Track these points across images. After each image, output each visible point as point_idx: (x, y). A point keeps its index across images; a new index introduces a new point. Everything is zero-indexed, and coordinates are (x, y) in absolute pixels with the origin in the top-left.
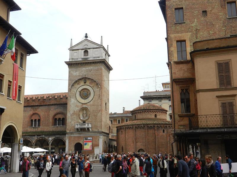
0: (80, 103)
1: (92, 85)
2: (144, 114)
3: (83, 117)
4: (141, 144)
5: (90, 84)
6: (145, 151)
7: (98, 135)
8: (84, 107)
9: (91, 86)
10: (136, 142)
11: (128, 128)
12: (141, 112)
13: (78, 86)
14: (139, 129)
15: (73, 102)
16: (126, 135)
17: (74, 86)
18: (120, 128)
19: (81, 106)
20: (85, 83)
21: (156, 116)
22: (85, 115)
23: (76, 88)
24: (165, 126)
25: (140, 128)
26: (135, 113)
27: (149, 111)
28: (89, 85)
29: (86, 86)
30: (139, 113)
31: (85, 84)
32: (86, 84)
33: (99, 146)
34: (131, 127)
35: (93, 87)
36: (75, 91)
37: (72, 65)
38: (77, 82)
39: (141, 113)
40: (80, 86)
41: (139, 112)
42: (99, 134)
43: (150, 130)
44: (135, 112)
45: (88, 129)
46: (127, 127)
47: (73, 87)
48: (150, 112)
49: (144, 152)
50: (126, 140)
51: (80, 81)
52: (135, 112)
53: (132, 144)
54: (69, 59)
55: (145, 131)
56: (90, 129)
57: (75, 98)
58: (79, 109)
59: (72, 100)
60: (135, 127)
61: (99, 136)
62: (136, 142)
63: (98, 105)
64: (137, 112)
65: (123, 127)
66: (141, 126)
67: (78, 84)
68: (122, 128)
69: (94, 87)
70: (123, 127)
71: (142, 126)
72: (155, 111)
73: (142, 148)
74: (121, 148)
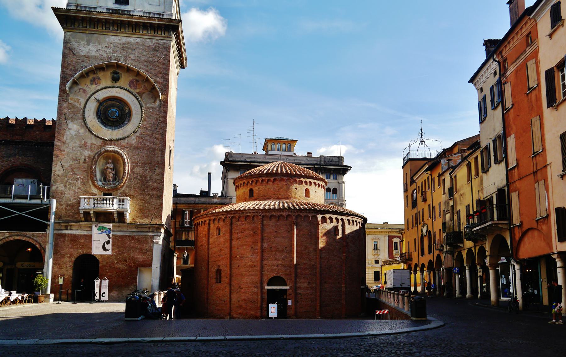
0: (95, 135)
1: (138, 91)
3: (105, 179)
5: (130, 86)
6: (288, 283)
7: (150, 234)
8: (108, 151)
9: (133, 91)
13: (94, 86)
15: (73, 132)
16: (231, 240)
17: (80, 87)
18: (212, 218)
19: (101, 146)
20: (115, 79)
21: (307, 192)
22: (112, 175)
23: (84, 91)
24: (340, 217)
28: (128, 87)
29: (117, 89)
31: (116, 85)
32: (118, 84)
33: (150, 265)
35: (138, 97)
36: (83, 101)
37: (76, 25)
38: (92, 76)
40: (99, 87)
42: (153, 231)
45: (121, 215)
47: (76, 88)
49: (286, 286)
51: (101, 74)
54: (67, 6)
56: (128, 216)
57: (81, 121)
58: (92, 154)
59: (71, 125)
61: (152, 237)
63: (154, 150)
65: (223, 217)
67: (93, 81)
69: (144, 96)
72: (308, 180)
74: (212, 273)
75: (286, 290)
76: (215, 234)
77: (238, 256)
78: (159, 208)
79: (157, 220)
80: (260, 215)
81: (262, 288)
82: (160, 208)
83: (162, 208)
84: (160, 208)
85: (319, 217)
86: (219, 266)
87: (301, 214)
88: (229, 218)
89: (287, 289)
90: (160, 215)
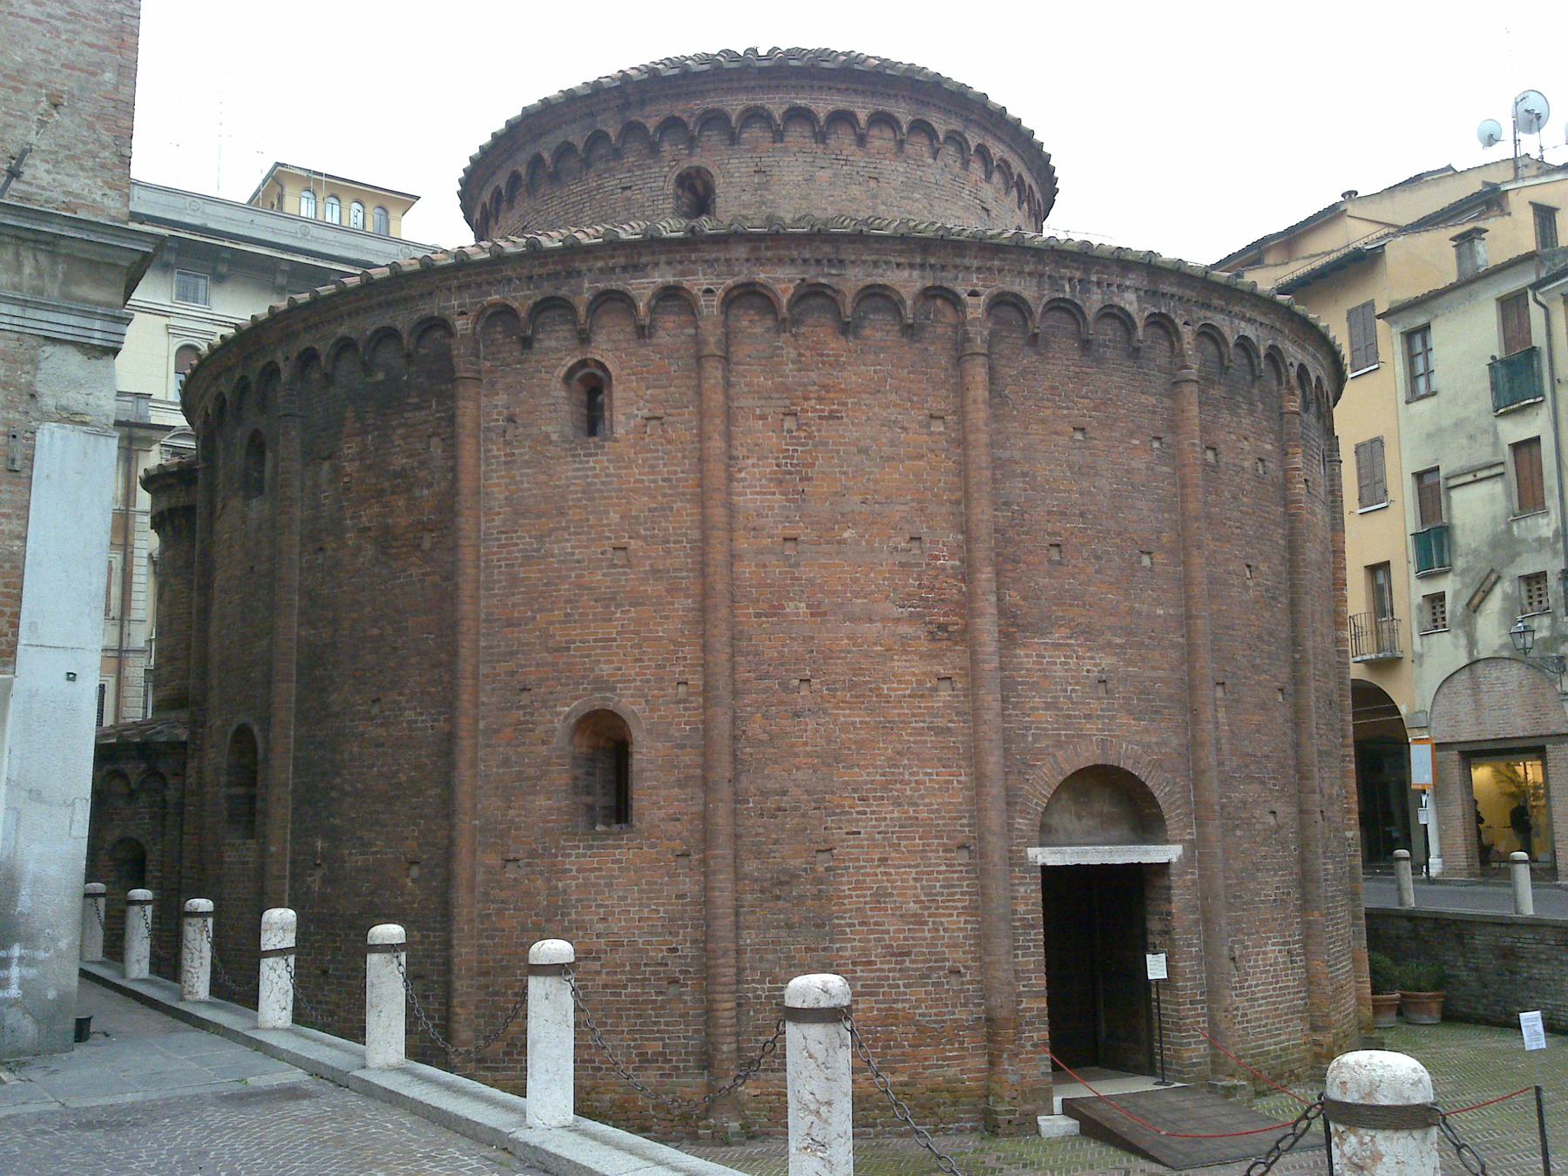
2: (895, 171)
4: (1107, 661)
10: (1012, 629)
11: (810, 293)
12: (842, 118)
14: (1062, 360)
18: (522, 299)
25: (1086, 345)
26: (714, 119)
27: (973, 139)
30: (797, 135)
34: (906, 282)
39: (843, 139)
41: (799, 115)
43: (1233, 411)
44: (698, 105)
46: (783, 280)
48: (977, 168)
50: (733, 557)
52: (698, 105)
53: (909, 668)
55: (1174, 426)
60: (1004, 302)
62: (1012, 629)
64: (755, 115)
65: (643, 288)
66: (1114, 314)
68: (619, 300)
70: (643, 288)
71: (1129, 302)
73: (1126, 755)
75: (1164, 867)
76: (553, 430)
77: (790, 608)
78: (94, 70)
79: (75, 186)
80: (974, 294)
81: (1015, 860)
82: (108, 76)
83: (128, 72)
84: (108, 76)
85: (1291, 364)
86: (602, 685)
87: (1218, 320)
88: (709, 291)
89: (1166, 865)
90: (106, 137)
